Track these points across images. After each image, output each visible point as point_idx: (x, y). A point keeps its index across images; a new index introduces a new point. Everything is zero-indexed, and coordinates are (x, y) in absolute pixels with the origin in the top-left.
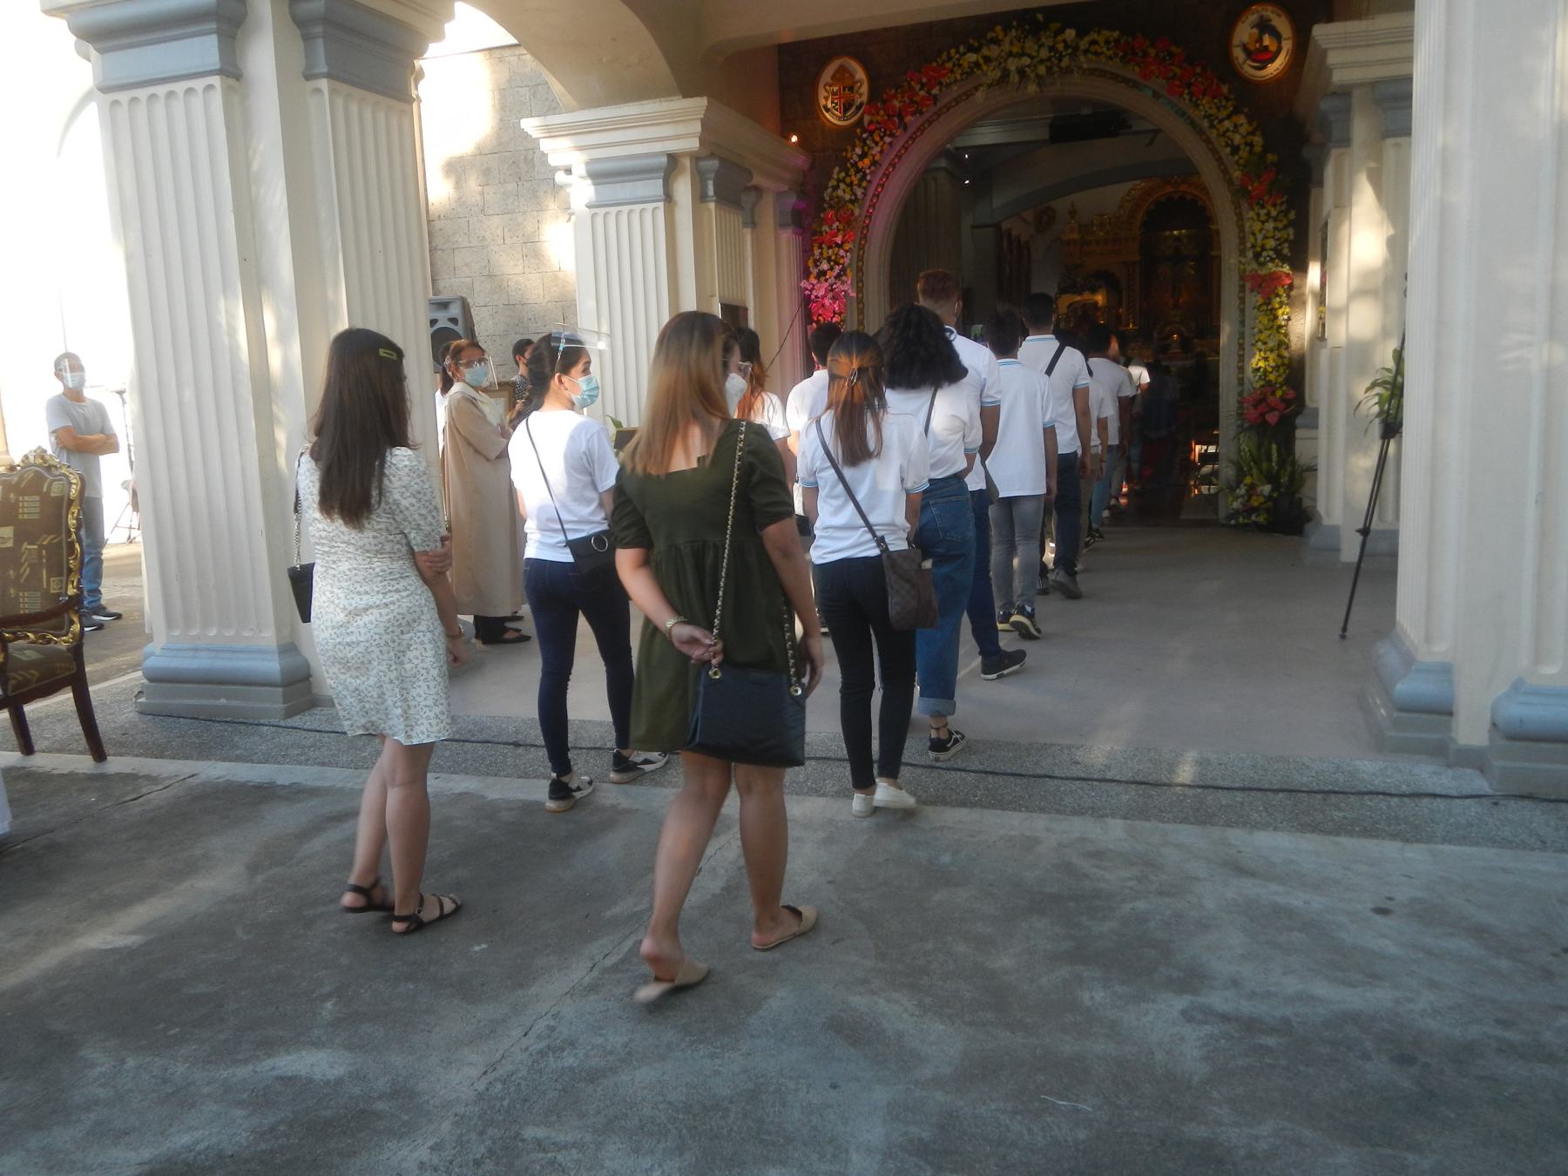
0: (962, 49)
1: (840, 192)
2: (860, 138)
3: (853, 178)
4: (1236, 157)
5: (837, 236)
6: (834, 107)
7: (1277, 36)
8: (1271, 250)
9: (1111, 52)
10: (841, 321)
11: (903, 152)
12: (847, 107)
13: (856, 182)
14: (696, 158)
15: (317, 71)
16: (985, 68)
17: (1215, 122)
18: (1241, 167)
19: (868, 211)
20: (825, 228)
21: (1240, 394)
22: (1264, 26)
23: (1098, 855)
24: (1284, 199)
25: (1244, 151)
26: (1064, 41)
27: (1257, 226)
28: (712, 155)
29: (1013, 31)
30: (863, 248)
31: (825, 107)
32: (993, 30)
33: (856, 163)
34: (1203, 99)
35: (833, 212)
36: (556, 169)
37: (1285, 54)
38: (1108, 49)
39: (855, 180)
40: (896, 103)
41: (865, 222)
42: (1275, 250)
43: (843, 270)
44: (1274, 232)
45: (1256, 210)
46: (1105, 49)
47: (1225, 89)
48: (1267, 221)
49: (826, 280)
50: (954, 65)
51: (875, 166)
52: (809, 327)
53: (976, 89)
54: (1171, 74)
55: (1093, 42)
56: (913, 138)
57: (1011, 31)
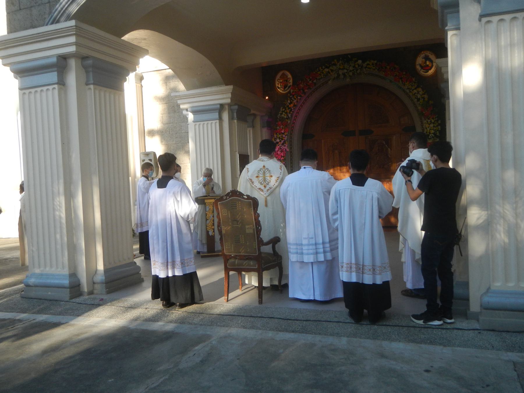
0: (323, 67)
1: (283, 115)
3: (287, 111)
4: (419, 102)
5: (282, 130)
6: (281, 87)
8: (432, 134)
10: (284, 159)
11: (305, 101)
12: (285, 87)
13: (288, 112)
14: (229, 105)
15: (90, 82)
16: (331, 73)
17: (411, 90)
19: (293, 122)
20: (278, 128)
23: (334, 350)
24: (436, 116)
25: (421, 101)
26: (358, 64)
27: (427, 125)
28: (236, 104)
30: (292, 134)
33: (288, 106)
34: (406, 82)
35: (281, 122)
36: (183, 109)
38: (373, 67)
39: (288, 111)
40: (302, 86)
41: (292, 125)
42: (434, 134)
44: (433, 127)
46: (372, 67)
47: (414, 80)
48: (430, 124)
49: (279, 145)
50: (321, 73)
53: (329, 80)
55: (368, 64)
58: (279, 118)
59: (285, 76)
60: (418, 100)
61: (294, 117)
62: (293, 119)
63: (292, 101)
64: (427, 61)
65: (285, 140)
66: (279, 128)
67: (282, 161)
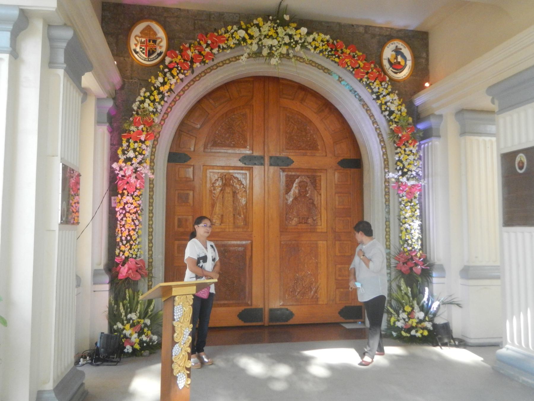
0: (235, 27)
1: (146, 105)
4: (392, 117)
5: (142, 135)
9: (324, 47)
10: (141, 195)
12: (150, 53)
16: (249, 42)
17: (381, 97)
18: (394, 123)
20: (133, 128)
21: (388, 254)
22: (398, 51)
26: (300, 34)
31: (135, 51)
34: (375, 81)
37: (408, 68)
40: (189, 53)
44: (413, 161)
46: (321, 45)
49: (132, 165)
52: (113, 198)
53: (242, 55)
54: (357, 66)
58: (135, 108)
59: (152, 32)
61: (162, 113)
63: (166, 80)
64: (399, 55)
65: (146, 156)
66: (134, 130)
67: (137, 198)
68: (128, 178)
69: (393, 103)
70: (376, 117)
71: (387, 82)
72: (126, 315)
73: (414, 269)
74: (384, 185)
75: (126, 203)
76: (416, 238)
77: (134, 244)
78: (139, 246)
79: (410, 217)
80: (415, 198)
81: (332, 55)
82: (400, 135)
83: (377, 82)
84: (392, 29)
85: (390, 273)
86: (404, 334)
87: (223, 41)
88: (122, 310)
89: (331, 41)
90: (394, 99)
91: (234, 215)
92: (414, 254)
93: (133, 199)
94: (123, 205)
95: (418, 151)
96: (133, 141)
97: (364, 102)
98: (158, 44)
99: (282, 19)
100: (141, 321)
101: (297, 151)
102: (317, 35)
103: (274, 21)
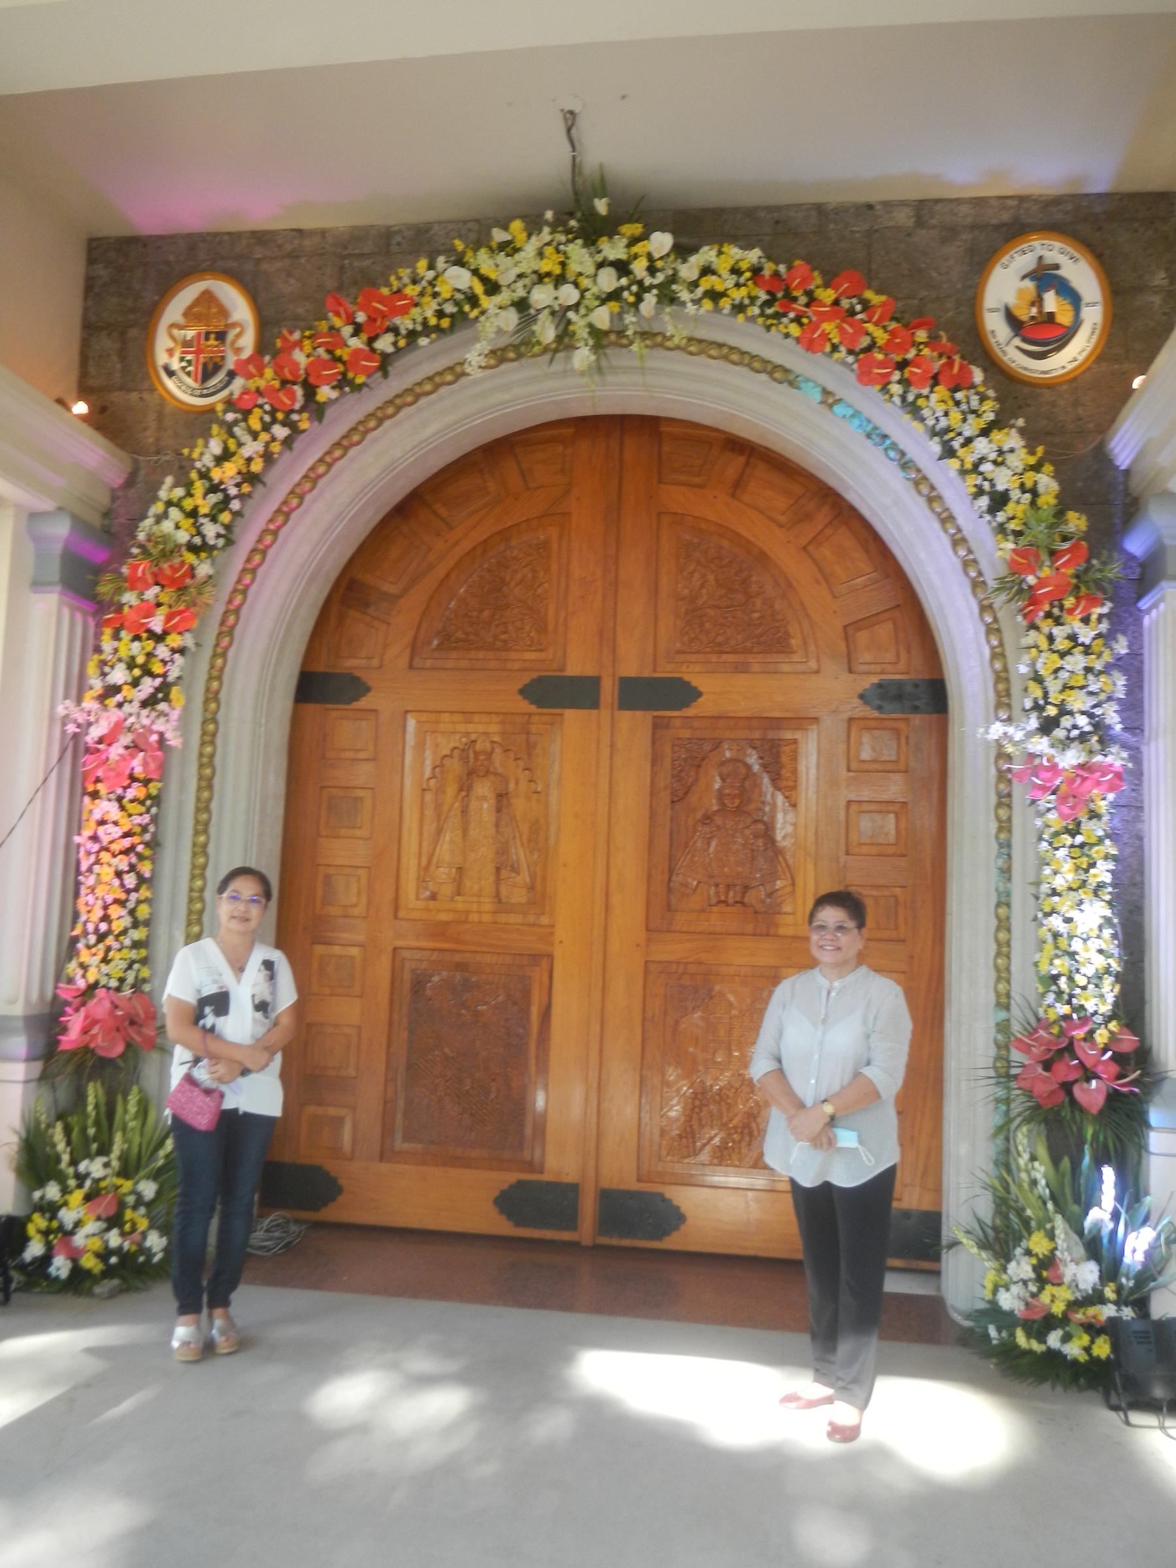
1: (167, 526)
2: (222, 423)
4: (1001, 517)
6: (183, 368)
7: (1074, 298)
9: (743, 291)
10: (149, 797)
12: (207, 373)
13: (204, 510)
16: (486, 302)
17: (956, 444)
18: (1011, 538)
19: (239, 581)
20: (129, 598)
21: (1003, 1027)
25: (1018, 506)
26: (650, 257)
27: (1046, 663)
29: (546, 230)
30: (224, 655)
32: (505, 228)
33: (209, 470)
38: (738, 285)
43: (164, 689)
45: (1046, 630)
49: (120, 705)
51: (252, 484)
54: (865, 341)
55: (707, 271)
56: (344, 445)
57: (540, 231)
59: (214, 310)
60: (999, 501)
62: (238, 563)
63: (232, 444)
65: (171, 679)
67: (134, 808)
68: (110, 745)
69: (1002, 463)
70: (961, 521)
71: (981, 389)
72: (74, 1162)
73: (1077, 1091)
74: (993, 771)
75: (102, 822)
76: (1090, 971)
77: (116, 945)
78: (134, 955)
79: (1070, 889)
80: (1094, 815)
81: (777, 316)
82: (1031, 580)
83: (941, 391)
84: (1022, 199)
85: (1007, 1101)
86: (1021, 1339)
87: (404, 311)
88: (61, 1146)
89: (768, 269)
90: (1006, 448)
91: (498, 869)
92: (1079, 1034)
93: (122, 808)
94: (92, 824)
95: (1107, 638)
96: (130, 637)
97: (919, 471)
98: (233, 343)
99: (590, 215)
100: (121, 1186)
101: (714, 658)
102: (713, 253)
103: (558, 225)
